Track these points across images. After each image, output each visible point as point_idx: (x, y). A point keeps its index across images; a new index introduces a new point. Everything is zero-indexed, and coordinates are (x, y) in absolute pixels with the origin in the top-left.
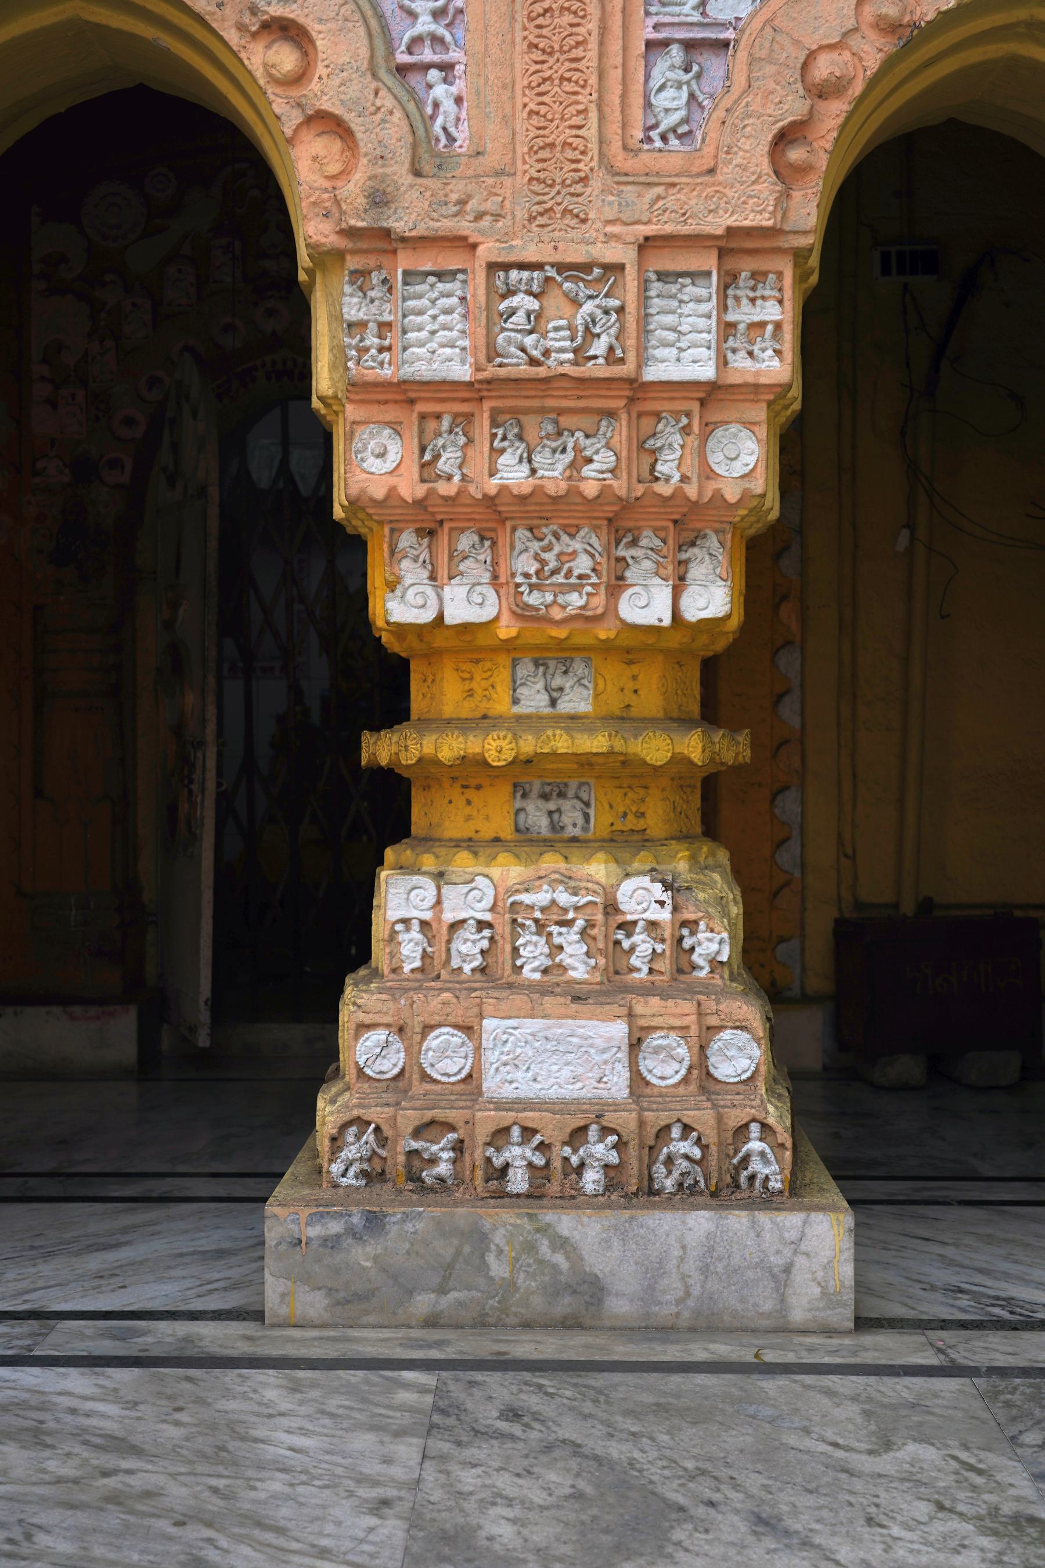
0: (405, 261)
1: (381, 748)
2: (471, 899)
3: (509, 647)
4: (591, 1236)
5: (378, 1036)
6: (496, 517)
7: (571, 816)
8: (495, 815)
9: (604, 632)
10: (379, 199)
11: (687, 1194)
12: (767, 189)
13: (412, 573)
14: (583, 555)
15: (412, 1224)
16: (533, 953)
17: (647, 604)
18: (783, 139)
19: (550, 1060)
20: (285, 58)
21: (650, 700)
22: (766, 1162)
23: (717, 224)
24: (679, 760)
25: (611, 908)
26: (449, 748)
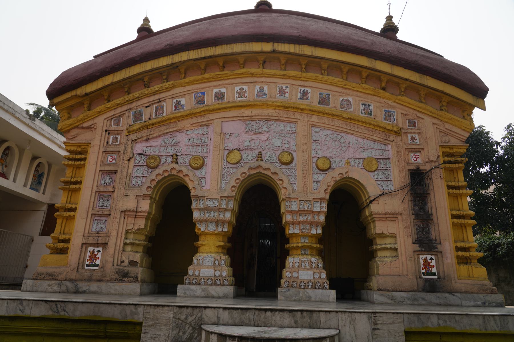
0: (292, 200)
1: (287, 246)
2: (297, 259)
3: (301, 236)
4: (310, 292)
5: (288, 273)
6: (299, 223)
7: (306, 252)
8: (299, 252)
9: (310, 234)
10: (289, 194)
11: (319, 288)
12: (324, 194)
13: (291, 228)
14: (308, 227)
15: (292, 290)
16: (303, 265)
17: (314, 232)
18: (325, 190)
19: (305, 275)
20: (281, 182)
21: (314, 241)
22: (327, 286)
23: (320, 197)
24: (317, 247)
25: (311, 261)
26: (295, 245)
